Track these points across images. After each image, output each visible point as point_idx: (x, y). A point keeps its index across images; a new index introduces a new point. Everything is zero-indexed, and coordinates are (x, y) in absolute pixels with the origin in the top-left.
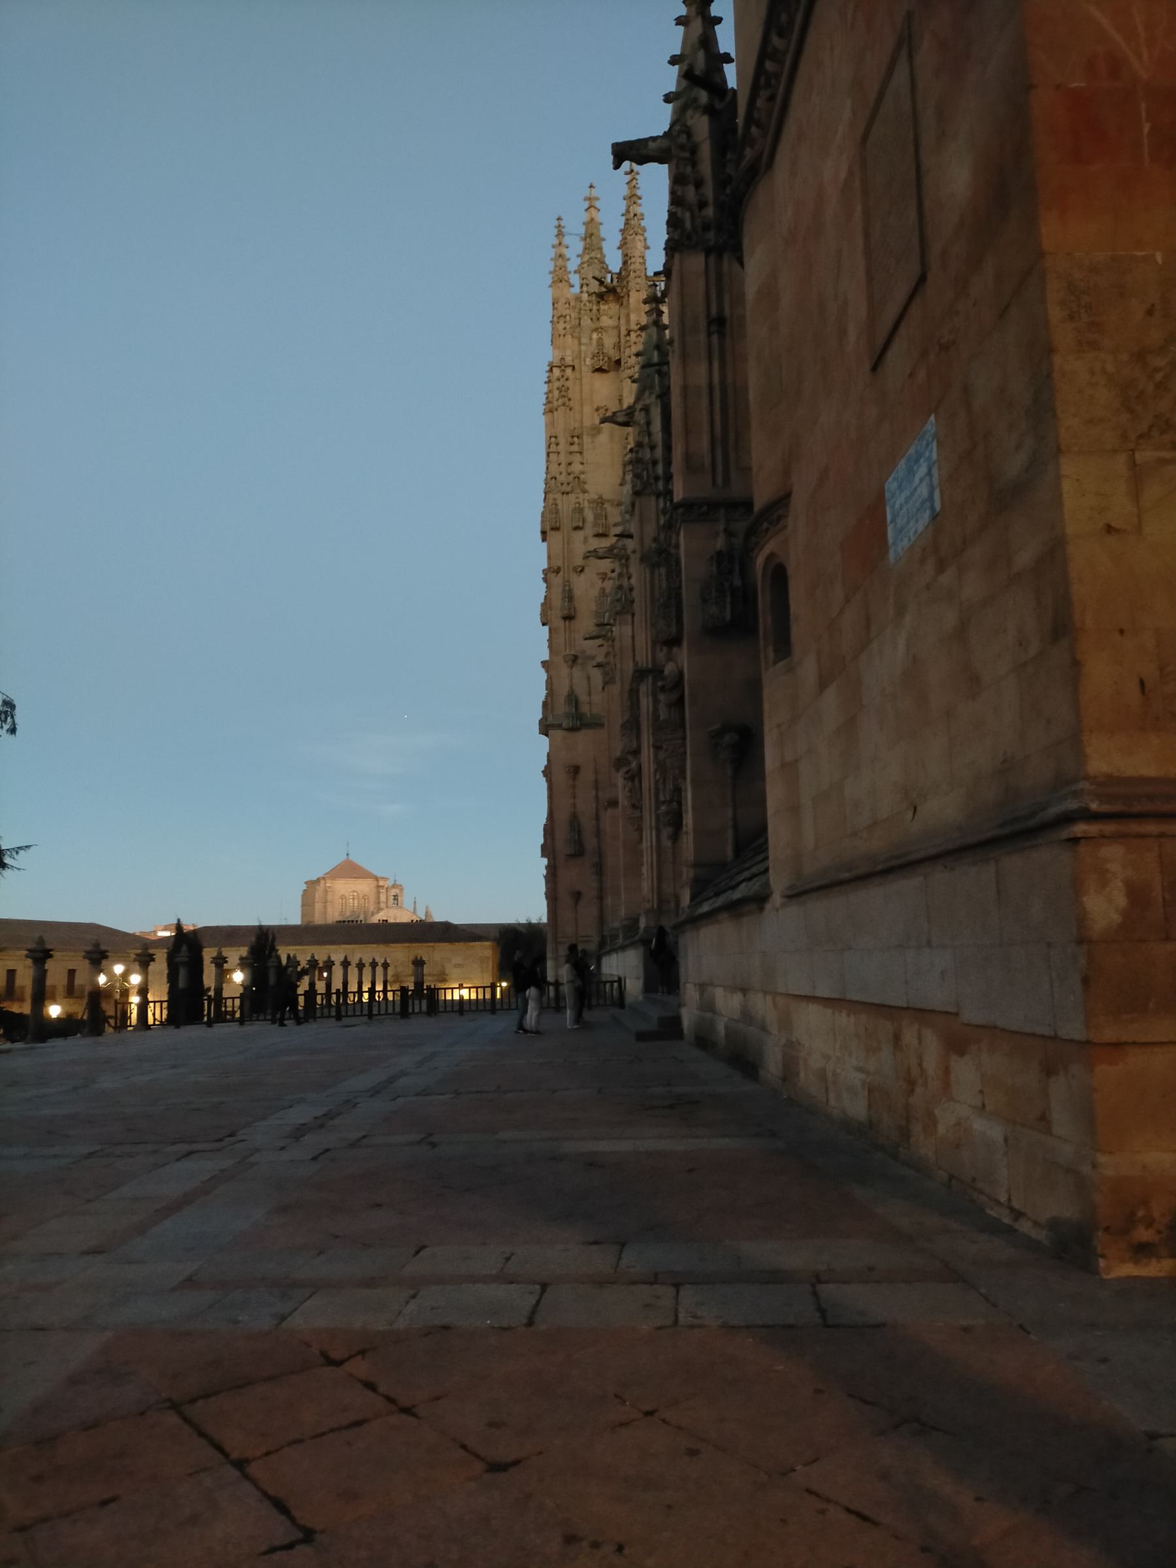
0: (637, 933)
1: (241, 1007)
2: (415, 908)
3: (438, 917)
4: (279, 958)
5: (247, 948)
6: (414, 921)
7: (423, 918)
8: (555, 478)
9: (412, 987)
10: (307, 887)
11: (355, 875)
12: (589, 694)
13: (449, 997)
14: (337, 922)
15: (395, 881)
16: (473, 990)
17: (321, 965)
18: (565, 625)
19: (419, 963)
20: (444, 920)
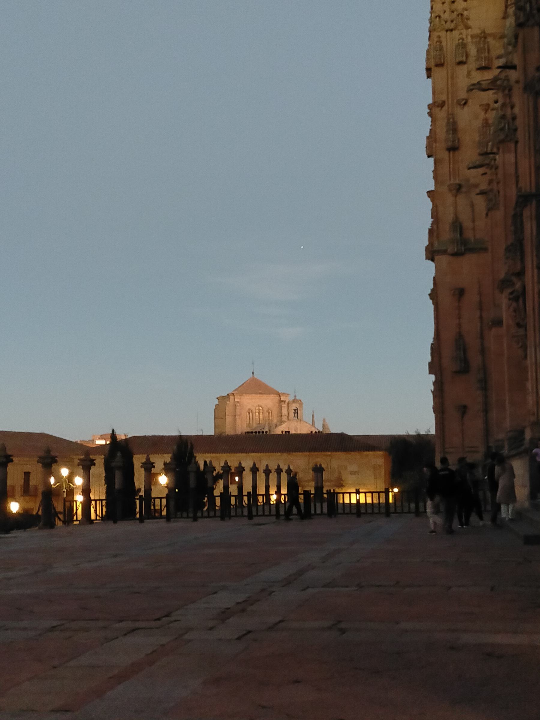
0: (522, 445)
1: (167, 506)
2: (313, 421)
3: (334, 429)
4: (196, 463)
5: (170, 455)
6: (314, 432)
7: (321, 430)
8: (440, 17)
9: (313, 492)
10: (219, 402)
11: (260, 392)
12: (473, 221)
13: (347, 501)
14: (245, 433)
15: (295, 396)
16: (369, 495)
17: (233, 471)
18: (449, 156)
19: (318, 470)
20: (340, 432)
